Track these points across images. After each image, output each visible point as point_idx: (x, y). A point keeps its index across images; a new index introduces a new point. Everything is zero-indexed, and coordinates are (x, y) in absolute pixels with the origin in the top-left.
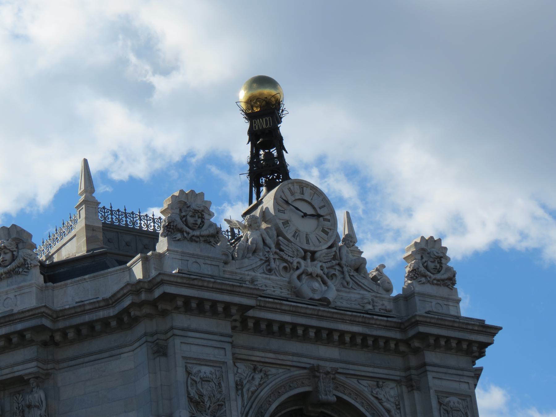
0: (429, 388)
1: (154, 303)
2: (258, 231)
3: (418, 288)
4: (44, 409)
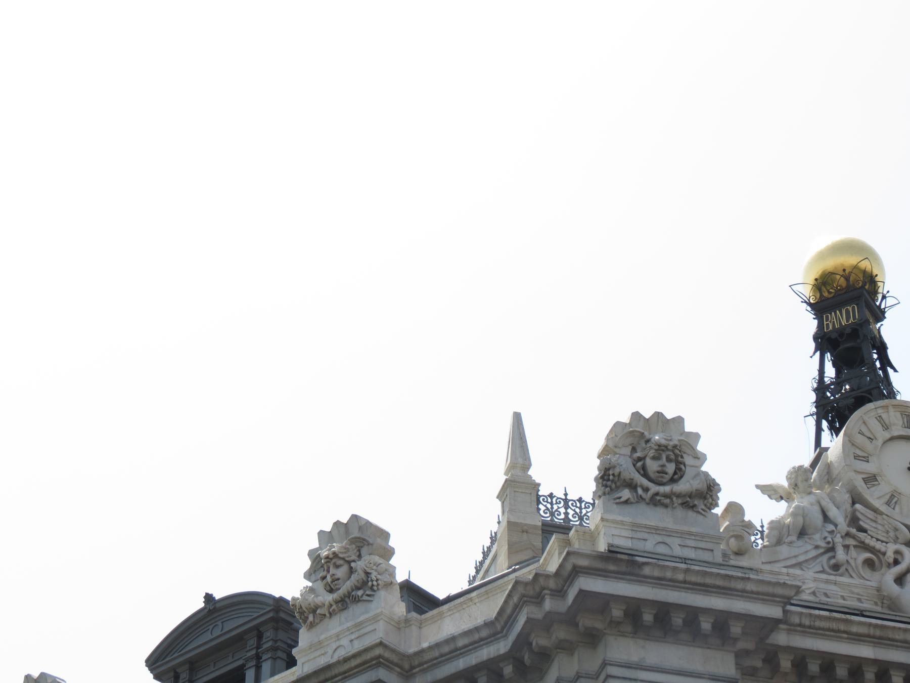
1: (570, 619)
2: (812, 496)
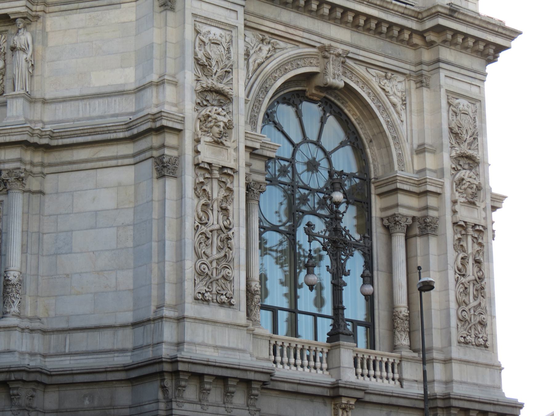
0: (440, 86)
4: (30, 53)
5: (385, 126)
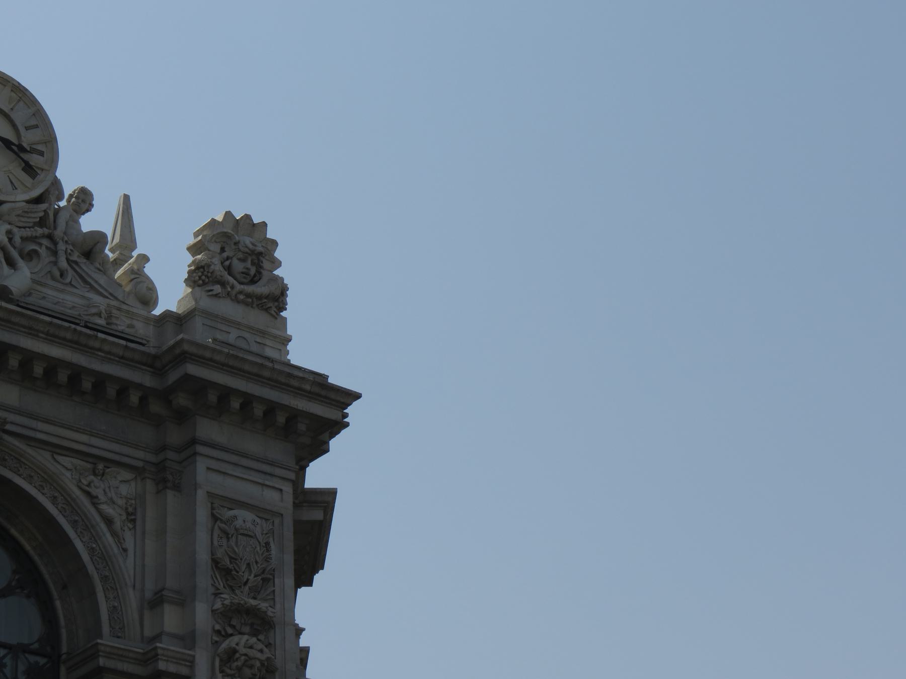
3: (206, 303)
5: (85, 557)
